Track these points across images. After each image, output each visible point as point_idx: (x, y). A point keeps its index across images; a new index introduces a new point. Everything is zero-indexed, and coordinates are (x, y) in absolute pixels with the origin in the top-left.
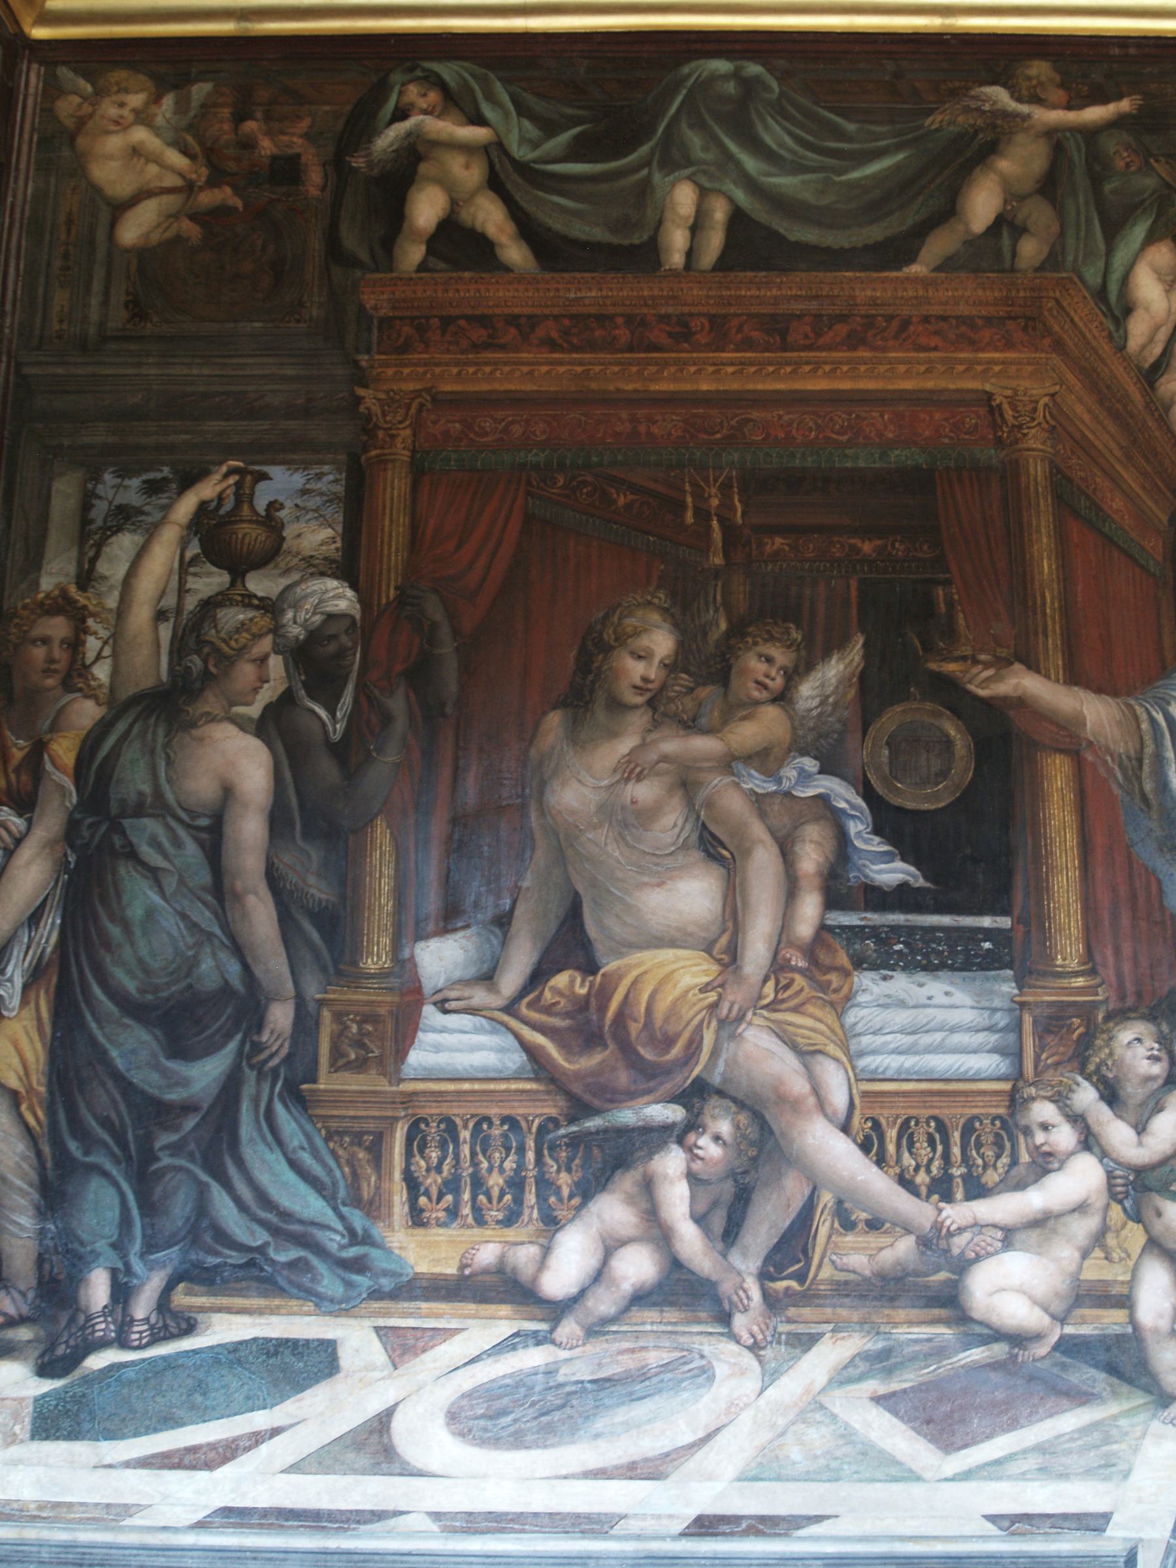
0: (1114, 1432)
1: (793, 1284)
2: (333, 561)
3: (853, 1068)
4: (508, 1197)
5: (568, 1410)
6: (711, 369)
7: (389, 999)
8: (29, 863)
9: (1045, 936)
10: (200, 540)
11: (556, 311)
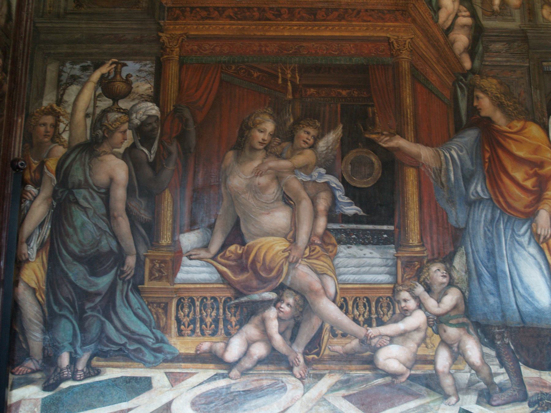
0: (428, 408)
1: (315, 356)
2: (150, 96)
3: (337, 280)
4: (213, 326)
5: (235, 402)
6: (288, 27)
7: (170, 255)
8: (39, 205)
9: (406, 233)
10: (102, 88)
11: (232, 6)
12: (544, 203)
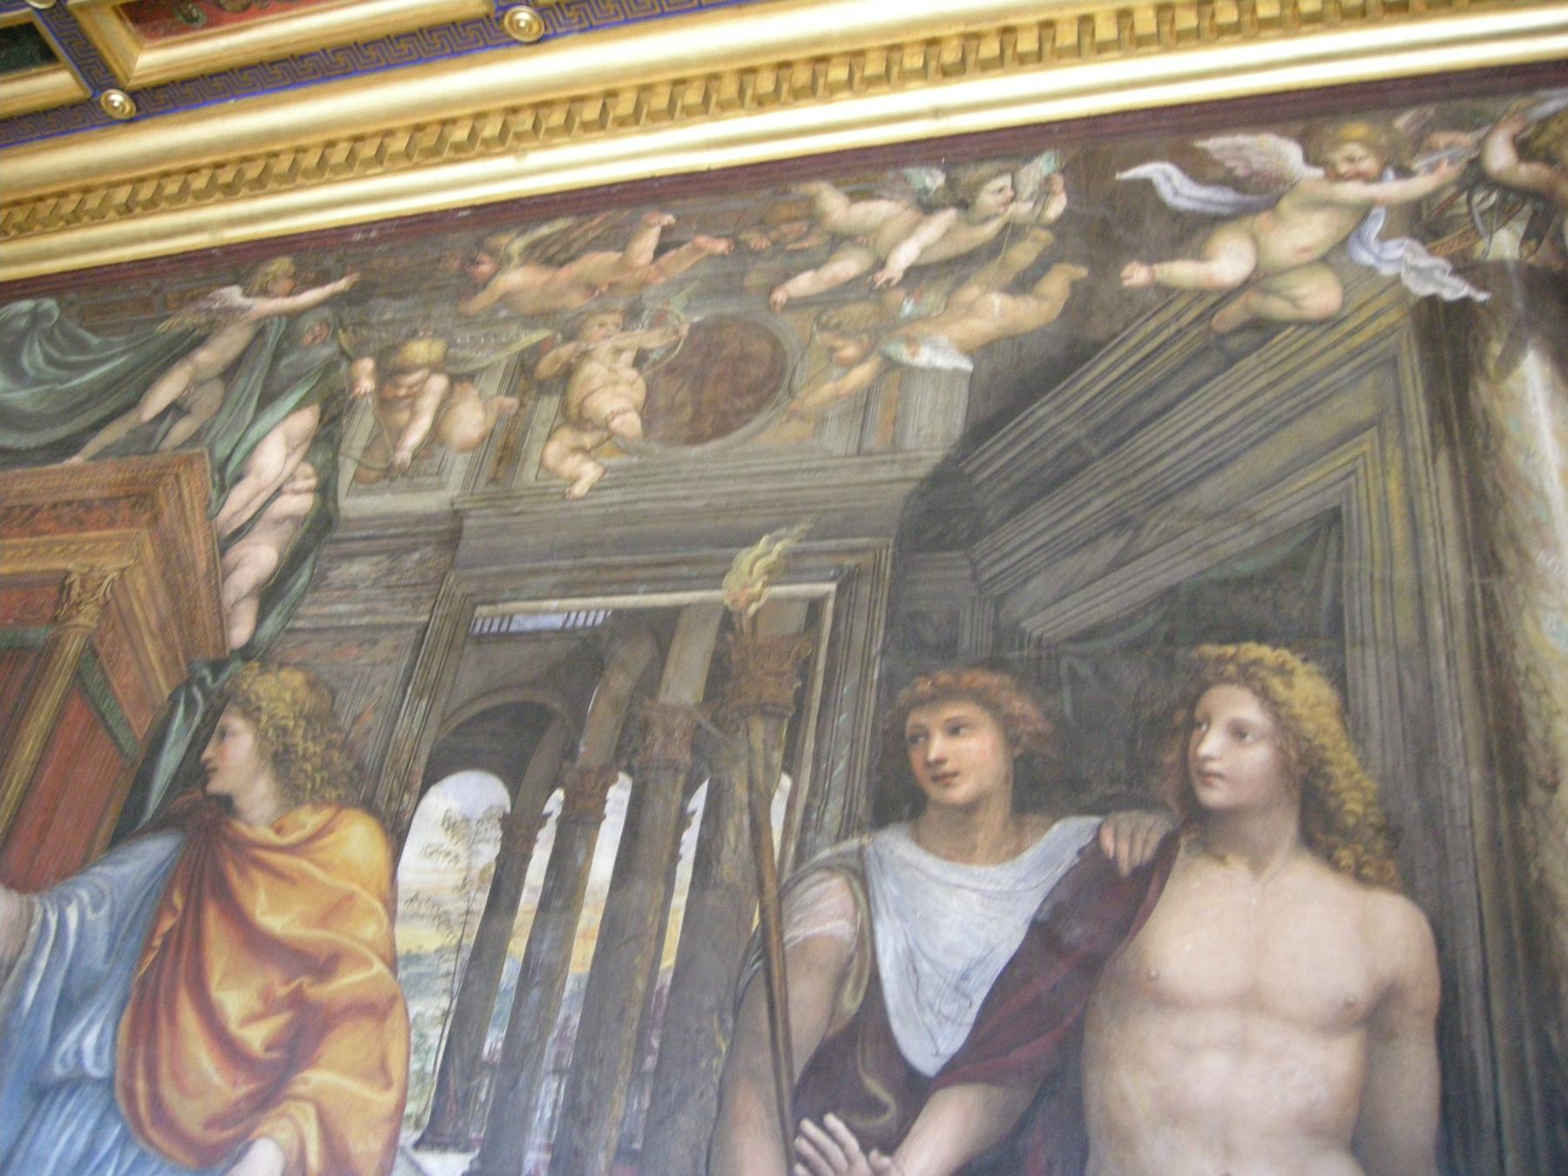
12: (282, 1115)
